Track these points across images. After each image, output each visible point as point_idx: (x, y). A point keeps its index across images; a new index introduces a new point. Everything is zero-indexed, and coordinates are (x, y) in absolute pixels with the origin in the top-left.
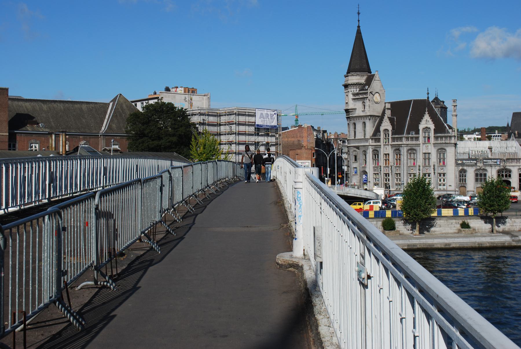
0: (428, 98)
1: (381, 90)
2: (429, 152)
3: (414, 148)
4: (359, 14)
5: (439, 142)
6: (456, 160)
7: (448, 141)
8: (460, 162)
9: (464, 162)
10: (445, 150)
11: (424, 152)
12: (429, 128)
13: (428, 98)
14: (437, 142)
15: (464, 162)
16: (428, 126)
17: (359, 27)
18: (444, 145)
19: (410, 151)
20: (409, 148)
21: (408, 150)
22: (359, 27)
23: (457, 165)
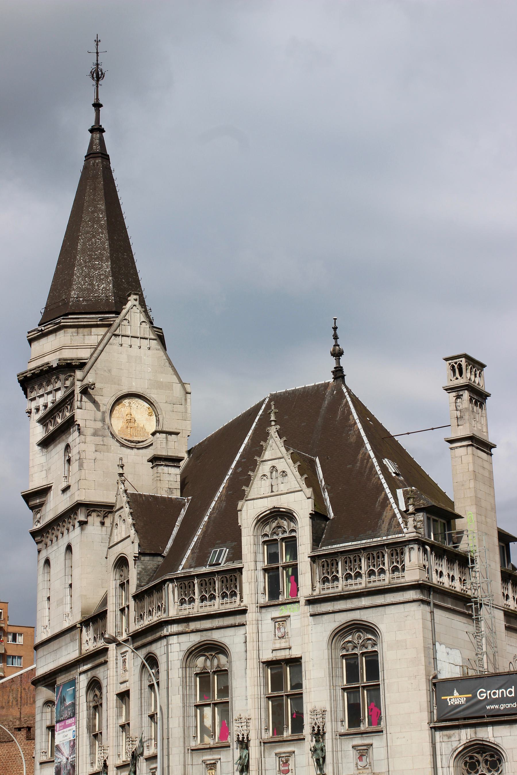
0: (339, 374)
1: (160, 386)
2: (295, 653)
3: (217, 636)
4: (97, 76)
5: (341, 586)
6: (438, 686)
7: (386, 579)
8: (456, 699)
9: (482, 694)
10: (369, 629)
11: (268, 656)
12: (289, 515)
13: (339, 374)
14: (331, 590)
15: (482, 694)
16: (284, 502)
17: (97, 130)
18: (365, 601)
19: (200, 661)
20: (195, 639)
21: (194, 652)
22: (97, 130)
23: (445, 721)
